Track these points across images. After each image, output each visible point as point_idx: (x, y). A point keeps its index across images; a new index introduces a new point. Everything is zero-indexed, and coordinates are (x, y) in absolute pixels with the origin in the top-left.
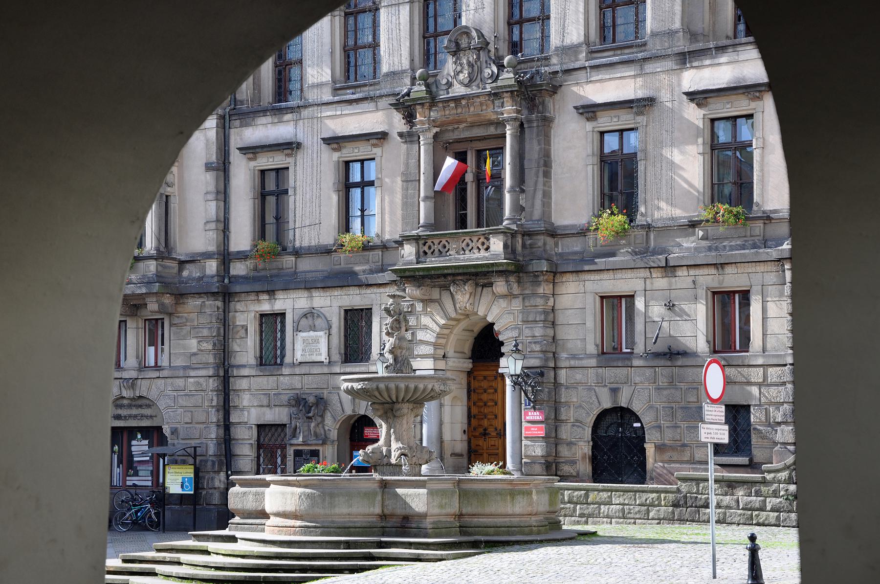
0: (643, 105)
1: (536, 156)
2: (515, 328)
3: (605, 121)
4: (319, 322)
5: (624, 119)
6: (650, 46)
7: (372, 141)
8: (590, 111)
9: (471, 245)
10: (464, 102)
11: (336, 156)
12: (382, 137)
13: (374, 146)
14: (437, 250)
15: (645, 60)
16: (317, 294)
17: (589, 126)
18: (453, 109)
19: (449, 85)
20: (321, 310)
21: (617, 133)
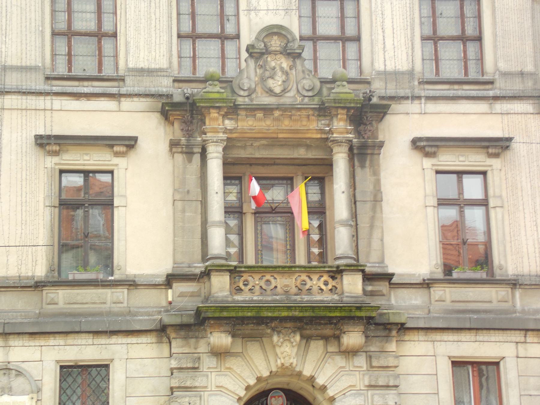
0: (498, 146)
1: (371, 187)
2: (360, 395)
3: (449, 160)
4: (18, 383)
5: (474, 159)
6: (497, 85)
7: (116, 149)
8: (425, 146)
9: (309, 283)
10: (277, 113)
11: (51, 162)
12: (129, 143)
13: (117, 154)
14: (257, 288)
15: (496, 98)
16: (21, 343)
17: (428, 163)
18: (260, 120)
19: (251, 92)
20: (24, 365)
21: (455, 176)
